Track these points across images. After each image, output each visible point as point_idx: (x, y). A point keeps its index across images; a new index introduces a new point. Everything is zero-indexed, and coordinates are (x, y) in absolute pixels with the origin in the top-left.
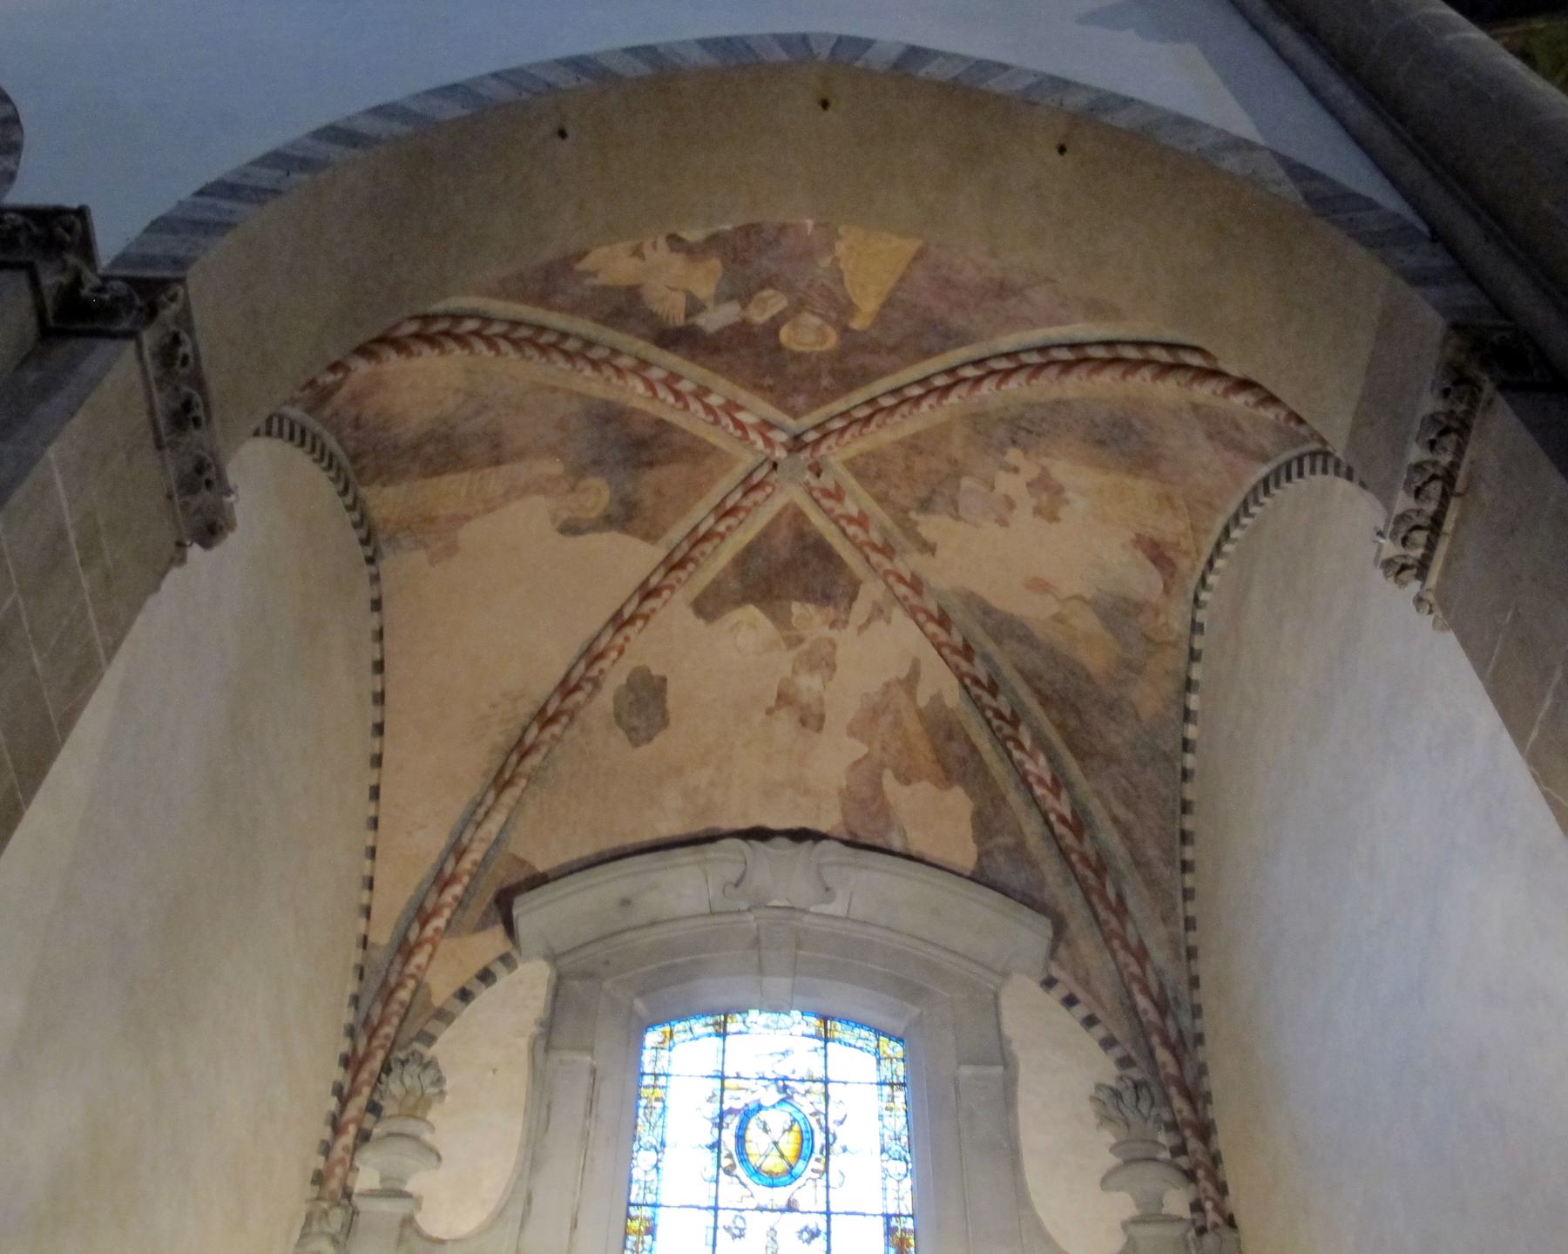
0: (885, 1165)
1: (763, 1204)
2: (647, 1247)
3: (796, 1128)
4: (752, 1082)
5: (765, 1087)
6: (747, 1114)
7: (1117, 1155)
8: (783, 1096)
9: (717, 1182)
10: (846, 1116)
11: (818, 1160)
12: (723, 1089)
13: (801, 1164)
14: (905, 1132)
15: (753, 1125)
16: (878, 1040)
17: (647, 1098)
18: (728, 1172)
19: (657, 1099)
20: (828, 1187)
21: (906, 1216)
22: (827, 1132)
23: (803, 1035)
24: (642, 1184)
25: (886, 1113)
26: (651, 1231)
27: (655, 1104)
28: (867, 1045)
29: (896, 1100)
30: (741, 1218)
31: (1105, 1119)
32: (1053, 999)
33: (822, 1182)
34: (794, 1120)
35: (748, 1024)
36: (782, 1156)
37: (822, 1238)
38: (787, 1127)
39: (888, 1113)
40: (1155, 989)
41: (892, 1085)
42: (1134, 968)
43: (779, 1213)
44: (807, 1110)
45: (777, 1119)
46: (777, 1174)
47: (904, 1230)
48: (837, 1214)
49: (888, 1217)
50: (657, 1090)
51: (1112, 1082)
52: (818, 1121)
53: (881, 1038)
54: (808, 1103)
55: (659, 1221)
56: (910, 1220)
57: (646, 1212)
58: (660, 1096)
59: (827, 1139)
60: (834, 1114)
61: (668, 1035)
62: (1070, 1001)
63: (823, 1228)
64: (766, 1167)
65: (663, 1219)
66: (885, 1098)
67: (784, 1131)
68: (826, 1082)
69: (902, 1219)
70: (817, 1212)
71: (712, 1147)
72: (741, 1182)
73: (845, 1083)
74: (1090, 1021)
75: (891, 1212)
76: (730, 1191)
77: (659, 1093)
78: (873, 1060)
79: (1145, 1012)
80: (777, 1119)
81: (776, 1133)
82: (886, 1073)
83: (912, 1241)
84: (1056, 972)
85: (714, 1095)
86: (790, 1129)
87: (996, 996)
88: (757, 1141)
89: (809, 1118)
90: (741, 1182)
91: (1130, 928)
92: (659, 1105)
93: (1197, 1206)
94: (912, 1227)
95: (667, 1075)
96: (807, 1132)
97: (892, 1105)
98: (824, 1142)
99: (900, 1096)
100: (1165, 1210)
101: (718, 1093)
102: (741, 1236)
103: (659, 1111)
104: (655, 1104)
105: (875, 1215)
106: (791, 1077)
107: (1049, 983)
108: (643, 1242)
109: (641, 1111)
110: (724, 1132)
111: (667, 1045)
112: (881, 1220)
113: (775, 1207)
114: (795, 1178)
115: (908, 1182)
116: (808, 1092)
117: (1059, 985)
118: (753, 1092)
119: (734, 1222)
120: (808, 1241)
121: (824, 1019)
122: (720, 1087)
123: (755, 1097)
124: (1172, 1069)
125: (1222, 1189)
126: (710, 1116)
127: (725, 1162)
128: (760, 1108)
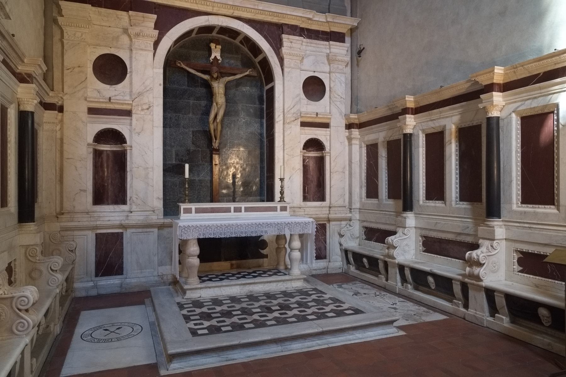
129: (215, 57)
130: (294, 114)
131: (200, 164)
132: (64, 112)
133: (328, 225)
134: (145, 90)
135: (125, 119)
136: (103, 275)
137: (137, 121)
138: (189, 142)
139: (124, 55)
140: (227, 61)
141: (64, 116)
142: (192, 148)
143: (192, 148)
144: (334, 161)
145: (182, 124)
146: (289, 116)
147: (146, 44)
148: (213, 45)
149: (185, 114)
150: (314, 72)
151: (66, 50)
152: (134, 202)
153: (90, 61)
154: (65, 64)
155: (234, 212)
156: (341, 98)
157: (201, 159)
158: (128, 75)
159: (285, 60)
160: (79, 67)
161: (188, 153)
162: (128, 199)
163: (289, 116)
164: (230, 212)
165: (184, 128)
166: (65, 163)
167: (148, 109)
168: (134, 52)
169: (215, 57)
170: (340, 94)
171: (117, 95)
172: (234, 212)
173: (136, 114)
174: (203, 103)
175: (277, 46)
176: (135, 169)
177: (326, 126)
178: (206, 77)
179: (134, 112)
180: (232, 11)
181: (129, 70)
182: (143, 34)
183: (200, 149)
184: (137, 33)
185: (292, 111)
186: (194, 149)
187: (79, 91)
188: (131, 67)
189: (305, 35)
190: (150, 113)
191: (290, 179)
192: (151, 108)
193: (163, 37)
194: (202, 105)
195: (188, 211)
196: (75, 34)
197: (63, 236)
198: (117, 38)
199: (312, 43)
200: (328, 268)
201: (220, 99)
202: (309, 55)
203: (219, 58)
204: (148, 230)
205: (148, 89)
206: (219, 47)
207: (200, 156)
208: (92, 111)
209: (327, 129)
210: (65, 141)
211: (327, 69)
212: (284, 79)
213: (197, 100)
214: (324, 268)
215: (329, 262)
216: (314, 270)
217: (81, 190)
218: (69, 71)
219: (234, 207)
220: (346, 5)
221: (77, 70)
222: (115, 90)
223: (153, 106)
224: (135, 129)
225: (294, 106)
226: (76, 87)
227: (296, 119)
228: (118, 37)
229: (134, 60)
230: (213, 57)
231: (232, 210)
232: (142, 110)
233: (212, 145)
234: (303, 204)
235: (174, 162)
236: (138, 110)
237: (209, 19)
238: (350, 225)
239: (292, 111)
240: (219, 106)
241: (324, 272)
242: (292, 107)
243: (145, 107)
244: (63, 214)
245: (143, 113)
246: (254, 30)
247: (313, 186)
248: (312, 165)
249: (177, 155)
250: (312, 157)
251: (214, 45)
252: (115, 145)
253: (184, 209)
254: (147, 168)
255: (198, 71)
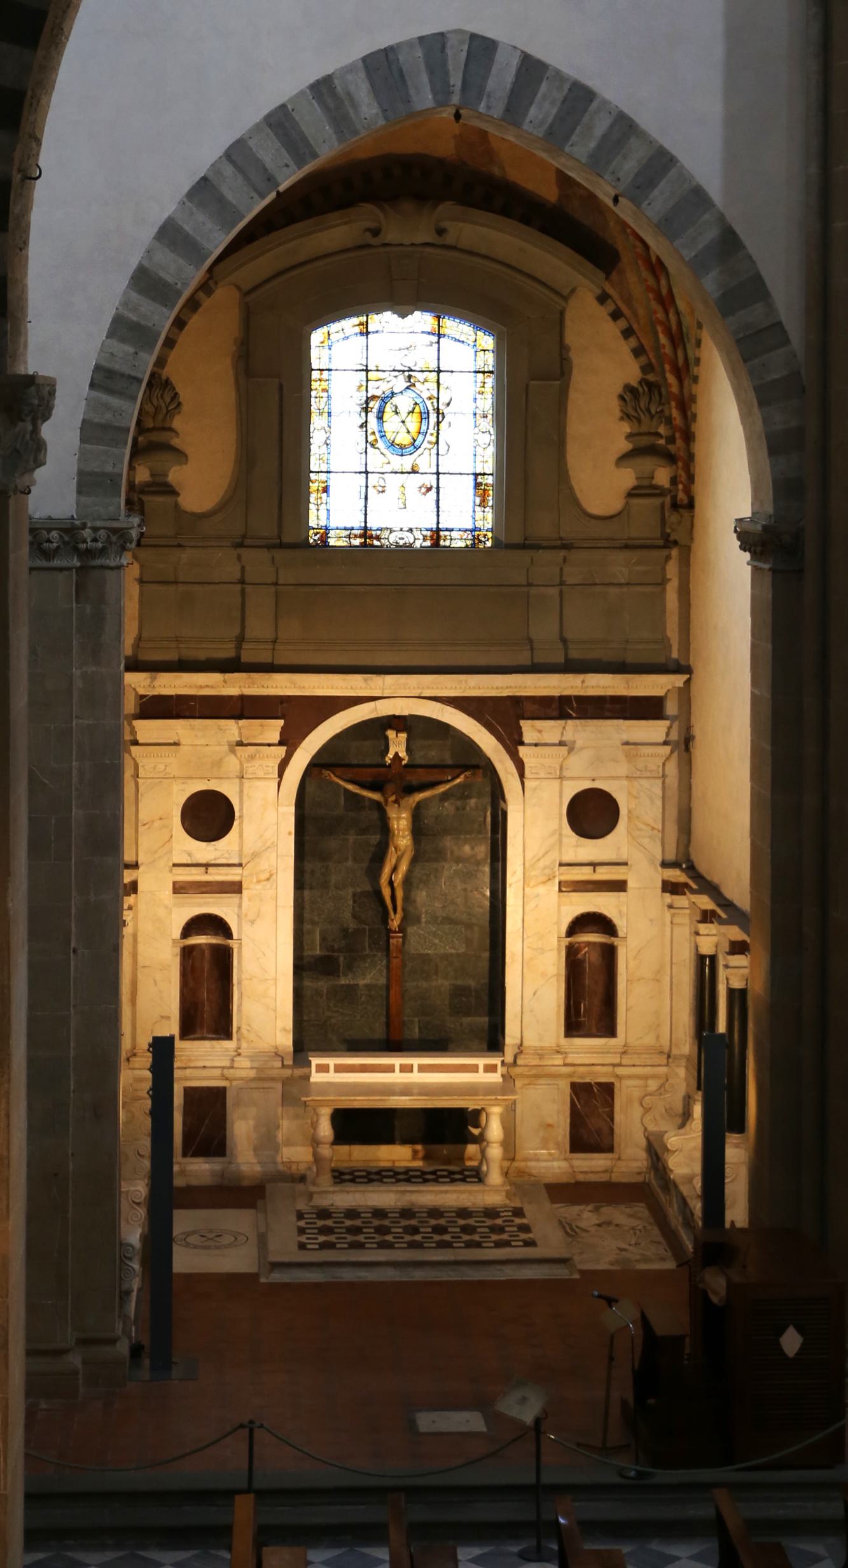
0: (476, 437)
1: (396, 469)
2: (324, 502)
3: (417, 410)
4: (387, 373)
5: (396, 377)
6: (384, 401)
7: (630, 442)
8: (409, 384)
9: (366, 452)
10: (451, 399)
11: (432, 434)
12: (367, 381)
13: (421, 438)
14: (491, 412)
15: (389, 408)
16: (476, 334)
17: (316, 389)
18: (373, 446)
19: (324, 390)
20: (438, 454)
21: (489, 475)
22: (438, 411)
23: (423, 332)
24: (317, 456)
25: (479, 396)
26: (326, 490)
27: (322, 394)
28: (468, 339)
29: (486, 385)
30: (383, 479)
31: (626, 416)
32: (602, 312)
33: (434, 451)
34: (416, 404)
35: (383, 324)
36: (408, 432)
37: (433, 492)
38: (411, 409)
39: (480, 396)
40: (674, 327)
41: (484, 372)
42: (660, 315)
43: (406, 475)
44: (425, 395)
45: (404, 402)
46: (405, 445)
47: (486, 485)
48: (444, 474)
49: (476, 475)
50: (323, 383)
51: (634, 383)
52: (432, 403)
53: (478, 333)
54: (426, 389)
55: (331, 483)
56: (491, 477)
57: (323, 477)
58: (324, 387)
59: (438, 417)
60: (444, 399)
61: (327, 335)
62: (616, 315)
63: (435, 485)
64: (397, 441)
65: (334, 481)
66: (479, 385)
67: (409, 413)
68: (439, 371)
69: (486, 477)
70: (431, 473)
71: (361, 426)
72: (382, 453)
73: (452, 372)
74: (627, 333)
75: (478, 472)
76: (375, 460)
77: (324, 385)
78: (472, 351)
79: (664, 346)
80: (404, 402)
81: (403, 414)
82: (480, 365)
83: (491, 492)
84: (610, 290)
85: (361, 386)
86: (414, 409)
87: (562, 314)
88: (392, 423)
89: (426, 400)
90: (382, 453)
91: (663, 282)
92: (325, 394)
93: (674, 481)
94: (491, 482)
95: (329, 370)
96: (425, 413)
97: (483, 389)
98: (436, 420)
99: (490, 381)
100: (654, 482)
101: (364, 383)
102: (383, 492)
103: (325, 399)
104: (322, 394)
105: (468, 474)
106: (413, 368)
107: (603, 299)
108: (321, 498)
109: (313, 400)
110: (369, 414)
111: (326, 344)
112: (472, 477)
113: (404, 471)
114: (417, 448)
115: (492, 450)
116: (426, 380)
117: (609, 301)
118: (388, 382)
119: (378, 482)
120: (424, 494)
121: (439, 318)
122: (365, 379)
123: (390, 385)
124: (675, 389)
125: (691, 478)
126: (359, 402)
127: (371, 438)
128: (393, 394)
129: (397, 754)
130: (545, 868)
131: (367, 955)
132: (138, 892)
133: (617, 1085)
134: (263, 848)
135: (233, 899)
136: (195, 1155)
137: (250, 900)
138: (347, 914)
139: (228, 789)
140: (422, 753)
141: (139, 899)
142: (352, 925)
143: (351, 925)
144: (635, 958)
145: (333, 881)
146: (533, 873)
147: (265, 768)
148: (391, 734)
149: (340, 863)
150: (594, 780)
151: (142, 795)
152: (244, 1038)
153: (178, 805)
154: (141, 816)
155: (401, 1071)
156: (653, 829)
157: (370, 947)
158: (236, 823)
159: (526, 766)
160: (161, 819)
161: (344, 936)
162: (234, 1030)
163: (533, 873)
164: (394, 1071)
165: (337, 888)
166: (139, 976)
167: (268, 879)
168: (246, 783)
169: (397, 754)
170: (651, 822)
171: (218, 858)
172: (401, 1071)
173: (247, 889)
174: (375, 839)
175: (512, 742)
176: (245, 983)
177: (619, 886)
178: (375, 796)
179: (244, 886)
180: (419, 691)
181: (237, 814)
182: (261, 755)
183: (367, 927)
184: (250, 754)
185: (541, 864)
186: (355, 927)
187: (160, 858)
188: (241, 809)
189: (572, 709)
190: (272, 886)
191: (534, 994)
192: (274, 877)
193: (296, 750)
194: (372, 843)
195: (323, 1069)
196: (155, 767)
197: (136, 1090)
198: (219, 763)
199: (586, 726)
200: (612, 1172)
201: (403, 840)
202: (582, 749)
203: (403, 754)
204: (266, 1085)
205: (268, 845)
206: (403, 736)
207: (367, 939)
208: (179, 889)
209: (622, 894)
210: (139, 940)
211: (623, 769)
212: (524, 801)
213: (361, 835)
214: (606, 1171)
215: (619, 1159)
216: (581, 1172)
217: (163, 1017)
218: (147, 826)
219: (401, 1066)
220: (669, 633)
221: (157, 823)
222: (216, 850)
223: (277, 873)
224: (246, 915)
225: (547, 853)
226: (155, 852)
227: (549, 879)
228: (221, 760)
229: (245, 798)
230: (391, 755)
231: (397, 1068)
232: (259, 882)
233: (388, 924)
234: (564, 1041)
235: (318, 952)
236: (252, 881)
237: (378, 708)
238: (665, 1090)
239: (541, 864)
240: (399, 853)
241: (604, 1178)
242: (540, 854)
243: (263, 876)
244: (135, 1055)
245: (259, 887)
246: (463, 714)
247: (590, 1004)
248: (593, 958)
249: (323, 939)
250: (594, 944)
251: (395, 732)
252: (214, 935)
253: (318, 1066)
254: (267, 980)
255: (363, 786)
